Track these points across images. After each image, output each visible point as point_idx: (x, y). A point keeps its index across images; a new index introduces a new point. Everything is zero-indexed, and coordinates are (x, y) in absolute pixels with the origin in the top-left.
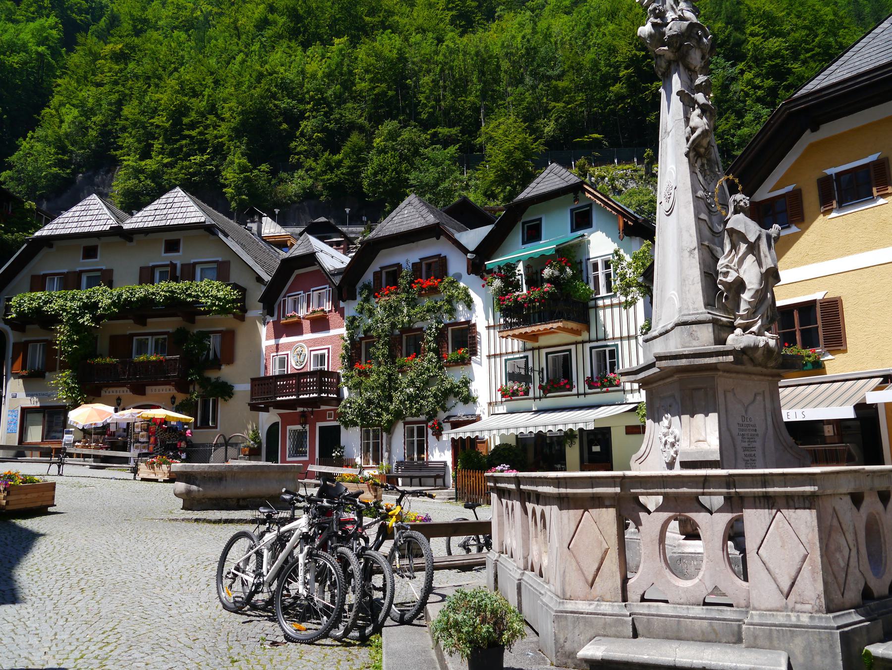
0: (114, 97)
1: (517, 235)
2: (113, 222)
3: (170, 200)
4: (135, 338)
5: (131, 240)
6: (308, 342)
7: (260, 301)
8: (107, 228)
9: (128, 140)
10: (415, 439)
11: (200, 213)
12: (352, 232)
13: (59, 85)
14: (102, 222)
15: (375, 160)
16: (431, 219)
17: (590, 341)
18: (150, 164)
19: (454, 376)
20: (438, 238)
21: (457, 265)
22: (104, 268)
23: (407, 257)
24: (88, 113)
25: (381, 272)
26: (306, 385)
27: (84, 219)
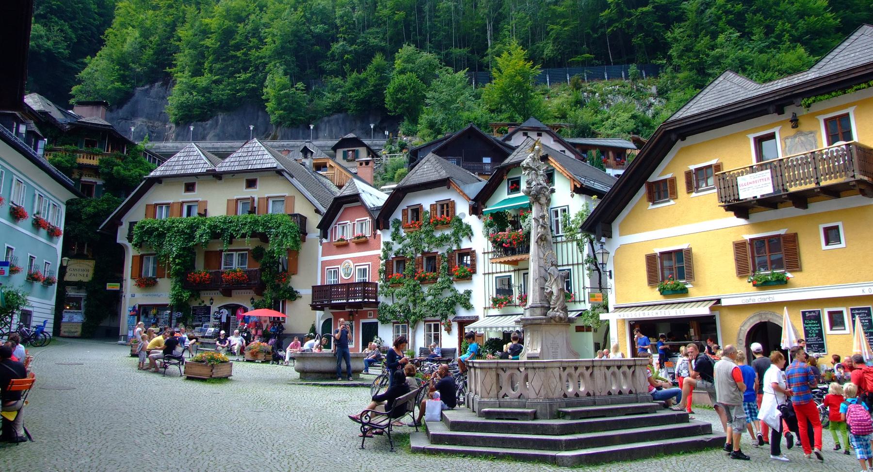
0: (168, 19)
2: (209, 166)
3: (250, 149)
5: (220, 179)
6: (354, 260)
7: (318, 227)
9: (182, 59)
10: (433, 333)
11: (273, 160)
12: (376, 145)
13: (120, 8)
15: (397, 80)
16: (444, 174)
18: (203, 81)
19: (461, 288)
20: (449, 188)
21: (462, 208)
23: (427, 202)
24: (146, 33)
26: (355, 292)
27: (186, 163)
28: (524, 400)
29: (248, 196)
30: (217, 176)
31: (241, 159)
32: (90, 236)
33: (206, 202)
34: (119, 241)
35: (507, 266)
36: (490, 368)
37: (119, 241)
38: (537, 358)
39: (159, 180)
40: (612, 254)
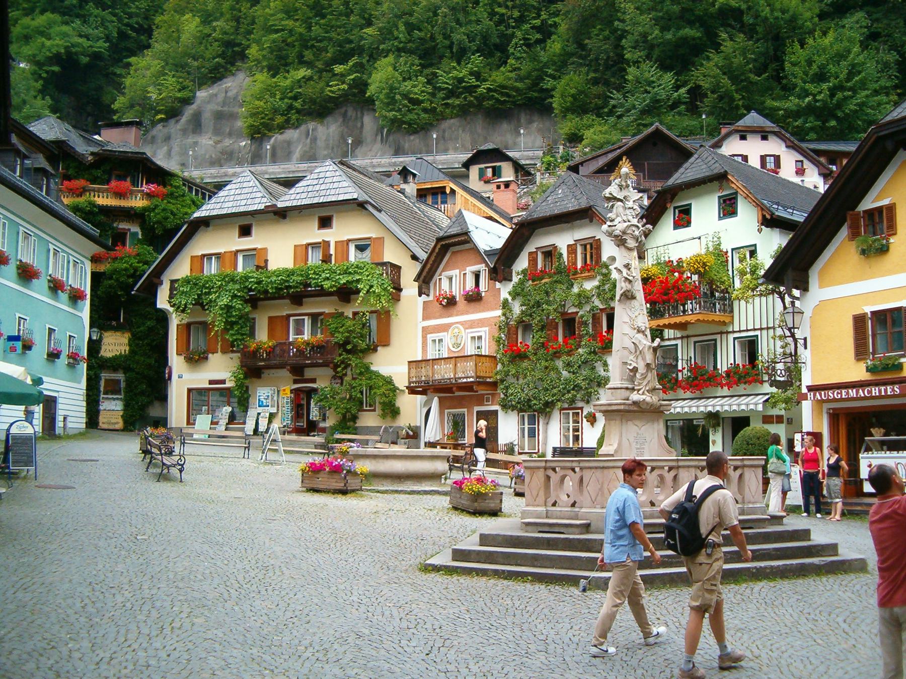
1: (668, 220)
3: (322, 175)
4: (292, 318)
8: (262, 207)
14: (257, 201)
17: (734, 332)
20: (591, 221)
22: (259, 247)
23: (562, 240)
25: (536, 252)
28: (577, 510)
29: (320, 240)
30: (282, 214)
31: (310, 189)
32: (120, 301)
33: (265, 250)
34: (160, 305)
35: (671, 331)
36: (538, 468)
37: (160, 305)
38: (612, 455)
39: (205, 222)
40: (808, 313)
